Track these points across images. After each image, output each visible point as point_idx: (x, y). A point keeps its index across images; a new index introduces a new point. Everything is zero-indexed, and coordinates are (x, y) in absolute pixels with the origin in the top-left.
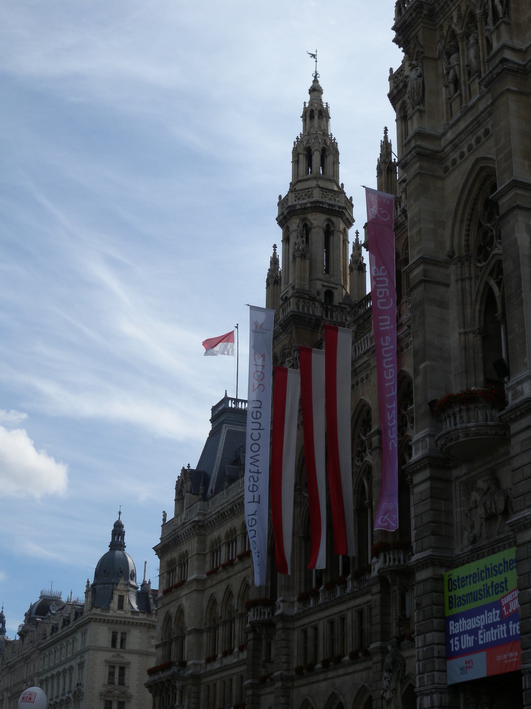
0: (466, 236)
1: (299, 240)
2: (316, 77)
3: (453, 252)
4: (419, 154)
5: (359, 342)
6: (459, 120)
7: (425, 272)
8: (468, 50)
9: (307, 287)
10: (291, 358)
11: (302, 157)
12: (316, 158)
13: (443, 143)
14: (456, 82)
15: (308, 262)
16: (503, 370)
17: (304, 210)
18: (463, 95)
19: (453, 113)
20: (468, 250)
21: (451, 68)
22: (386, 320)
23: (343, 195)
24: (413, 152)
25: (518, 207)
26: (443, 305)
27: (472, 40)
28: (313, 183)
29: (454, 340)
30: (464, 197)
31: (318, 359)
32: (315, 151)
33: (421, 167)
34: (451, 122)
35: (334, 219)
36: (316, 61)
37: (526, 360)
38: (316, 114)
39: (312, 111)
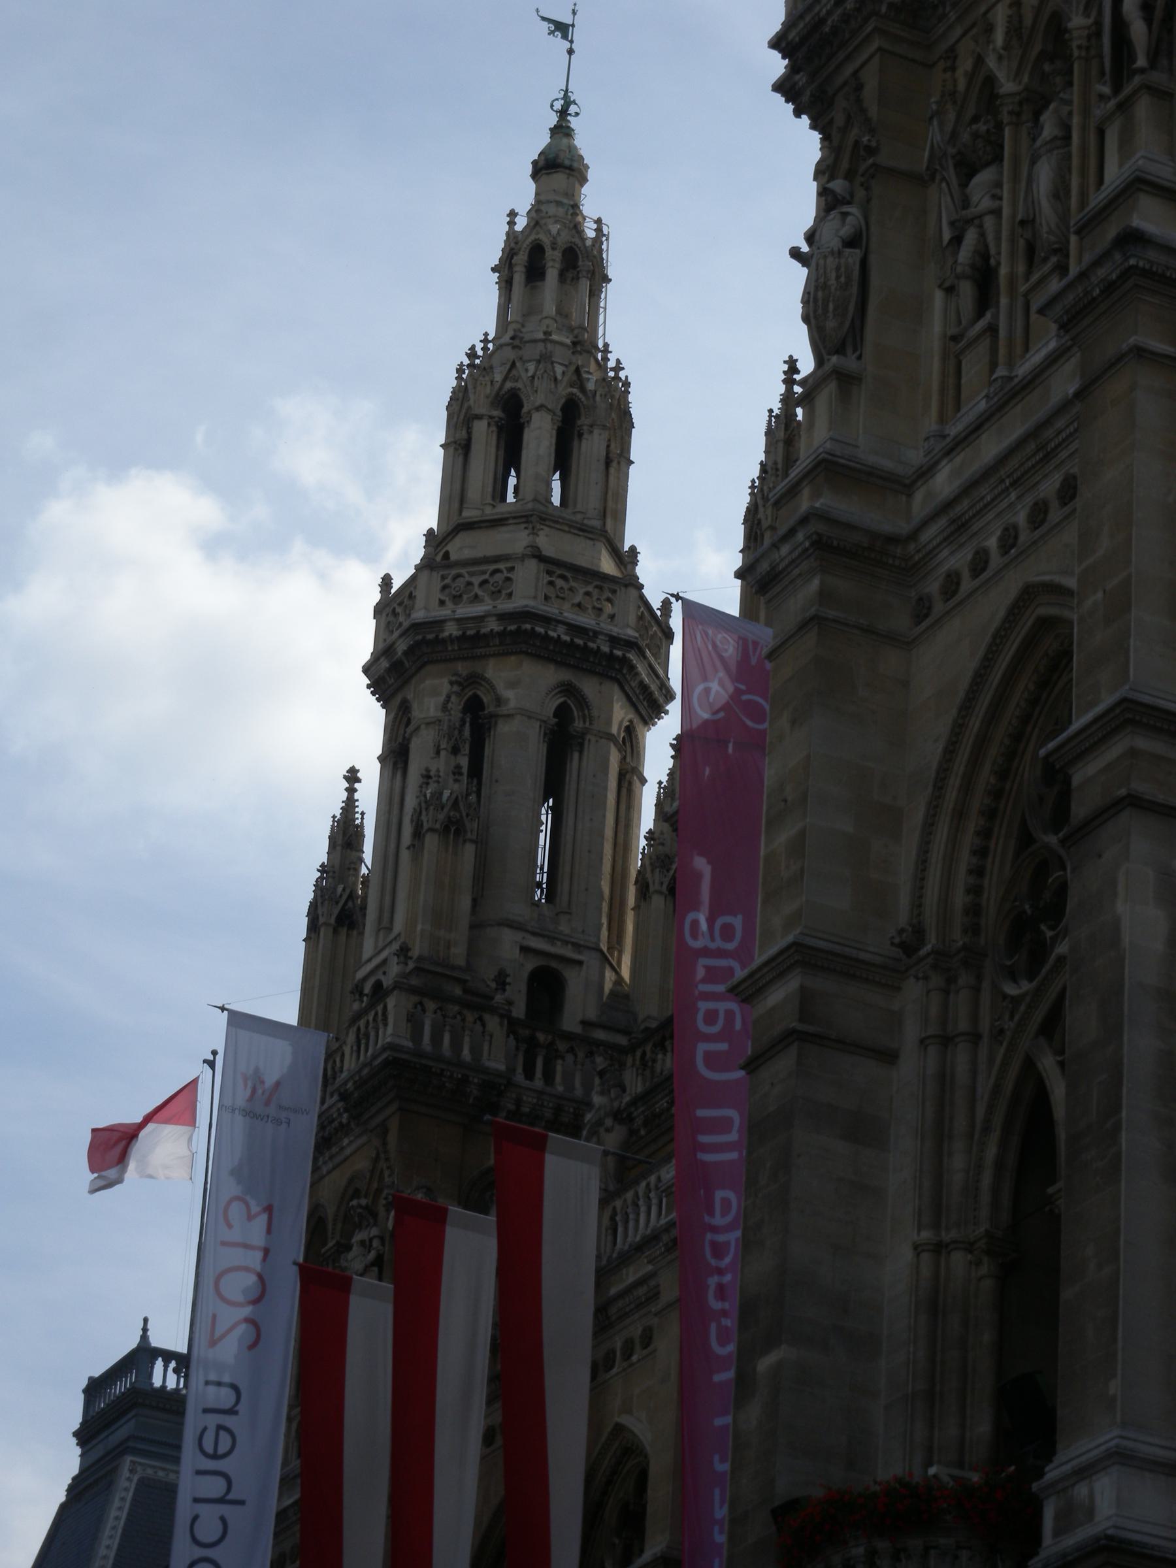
0: (970, 872)
1: (441, 765)
2: (563, 113)
3: (919, 932)
4: (820, 544)
5: (629, 1195)
6: (977, 427)
7: (805, 997)
8: (1033, 162)
9: (458, 954)
10: (374, 1231)
11: (481, 429)
12: (539, 437)
13: (920, 503)
14: (984, 278)
15: (469, 852)
16: (1029, 1419)
17: (473, 643)
18: (1002, 333)
19: (963, 396)
20: (974, 929)
21: (969, 222)
22: (723, 1125)
23: (633, 592)
24: (800, 536)
25: (1135, 802)
26: (865, 1130)
27: (1049, 130)
28: (515, 540)
29: (896, 1268)
30: (975, 724)
31: (469, 1254)
32: (539, 409)
33: (824, 596)
34: (955, 429)
35: (589, 687)
36: (571, 52)
37: (1114, 1387)
38: (554, 256)
39: (537, 250)
